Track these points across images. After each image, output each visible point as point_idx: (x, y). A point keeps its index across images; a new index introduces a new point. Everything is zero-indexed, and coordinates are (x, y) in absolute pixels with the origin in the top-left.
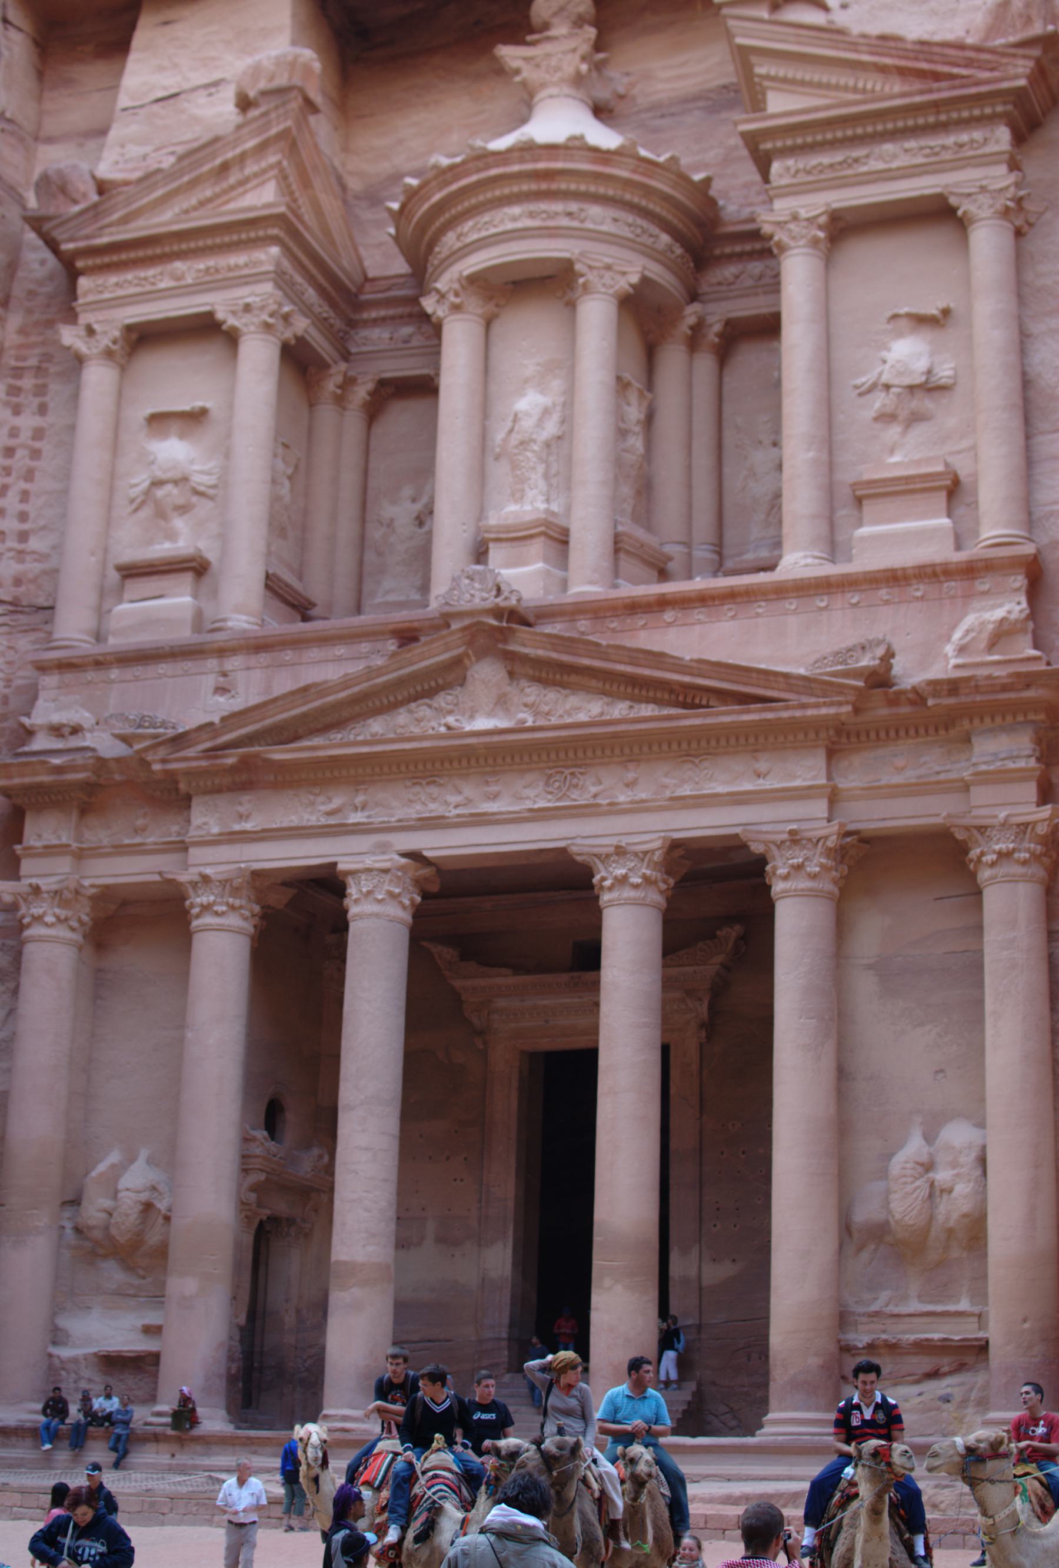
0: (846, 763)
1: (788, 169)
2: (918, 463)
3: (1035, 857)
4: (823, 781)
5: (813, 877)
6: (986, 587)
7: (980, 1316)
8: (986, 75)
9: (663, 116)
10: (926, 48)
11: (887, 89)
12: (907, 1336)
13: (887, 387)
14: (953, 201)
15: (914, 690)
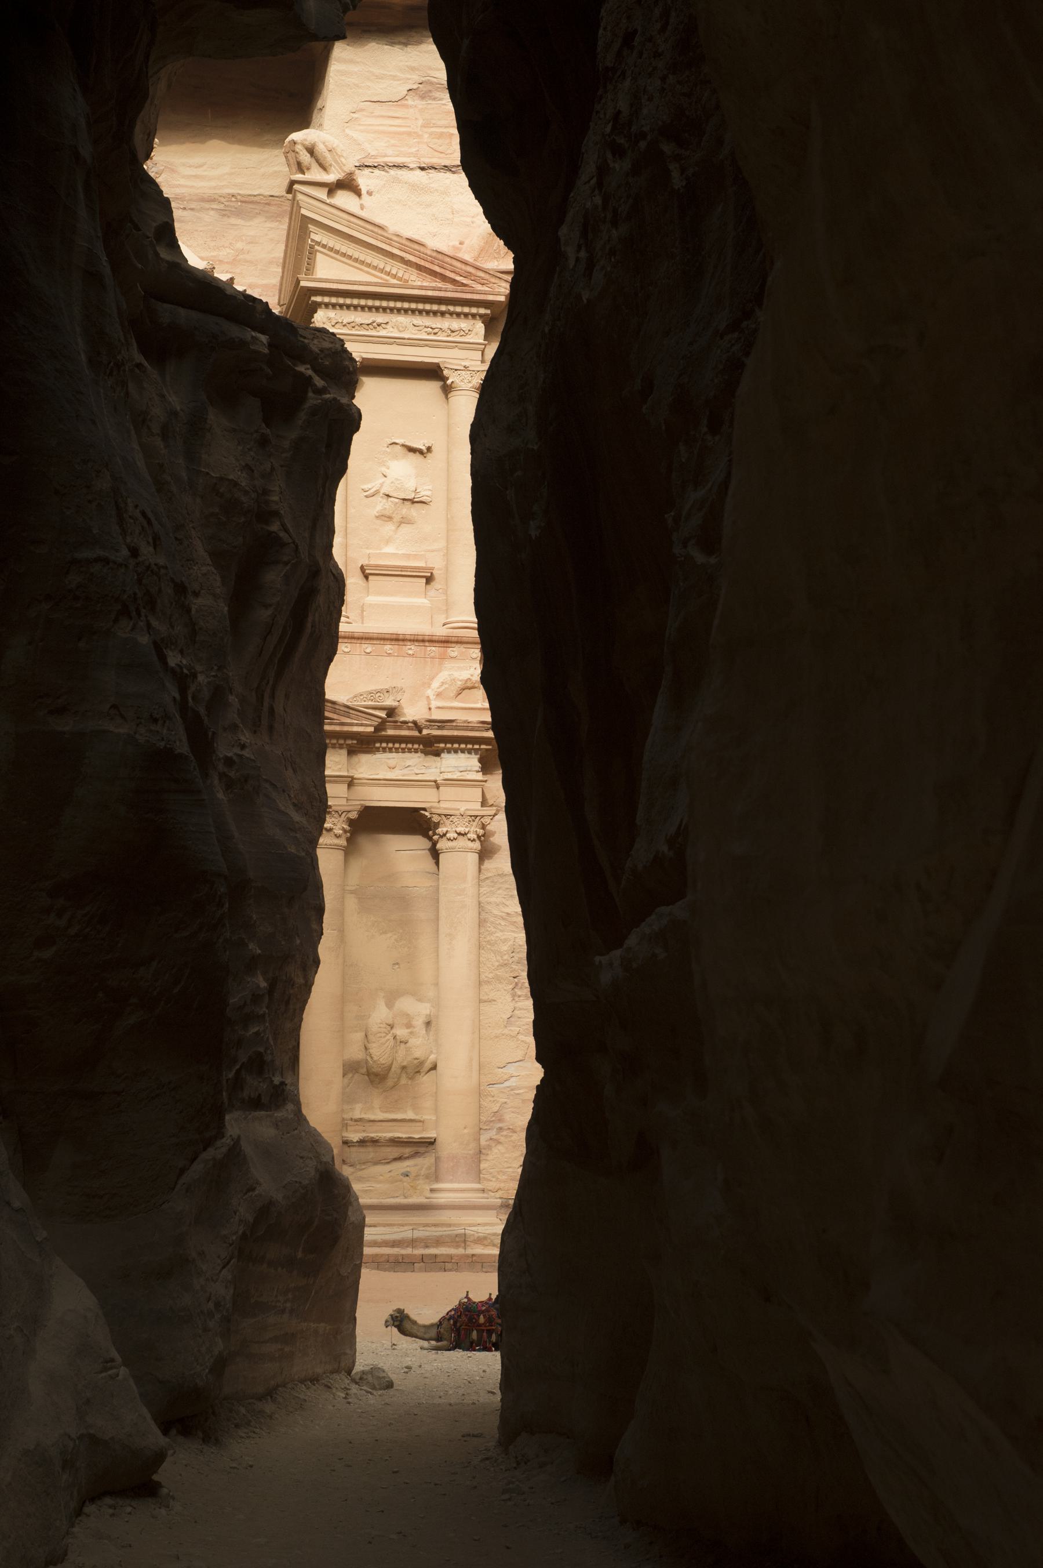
0: (355, 759)
1: (330, 319)
2: (407, 556)
3: (479, 837)
4: (346, 774)
5: (338, 836)
6: (453, 654)
7: (423, 1122)
8: (479, 287)
9: (185, 209)
10: (440, 256)
11: (406, 277)
12: (384, 1135)
13: (388, 496)
14: (446, 372)
15: (415, 723)
